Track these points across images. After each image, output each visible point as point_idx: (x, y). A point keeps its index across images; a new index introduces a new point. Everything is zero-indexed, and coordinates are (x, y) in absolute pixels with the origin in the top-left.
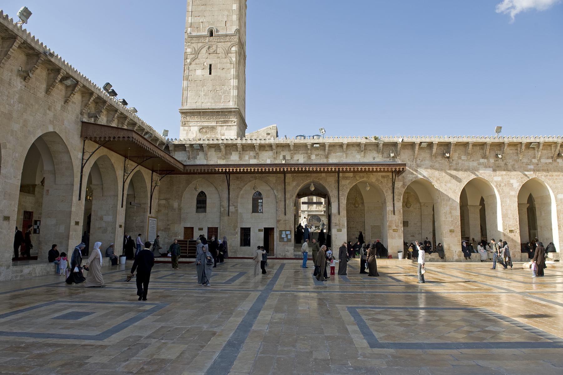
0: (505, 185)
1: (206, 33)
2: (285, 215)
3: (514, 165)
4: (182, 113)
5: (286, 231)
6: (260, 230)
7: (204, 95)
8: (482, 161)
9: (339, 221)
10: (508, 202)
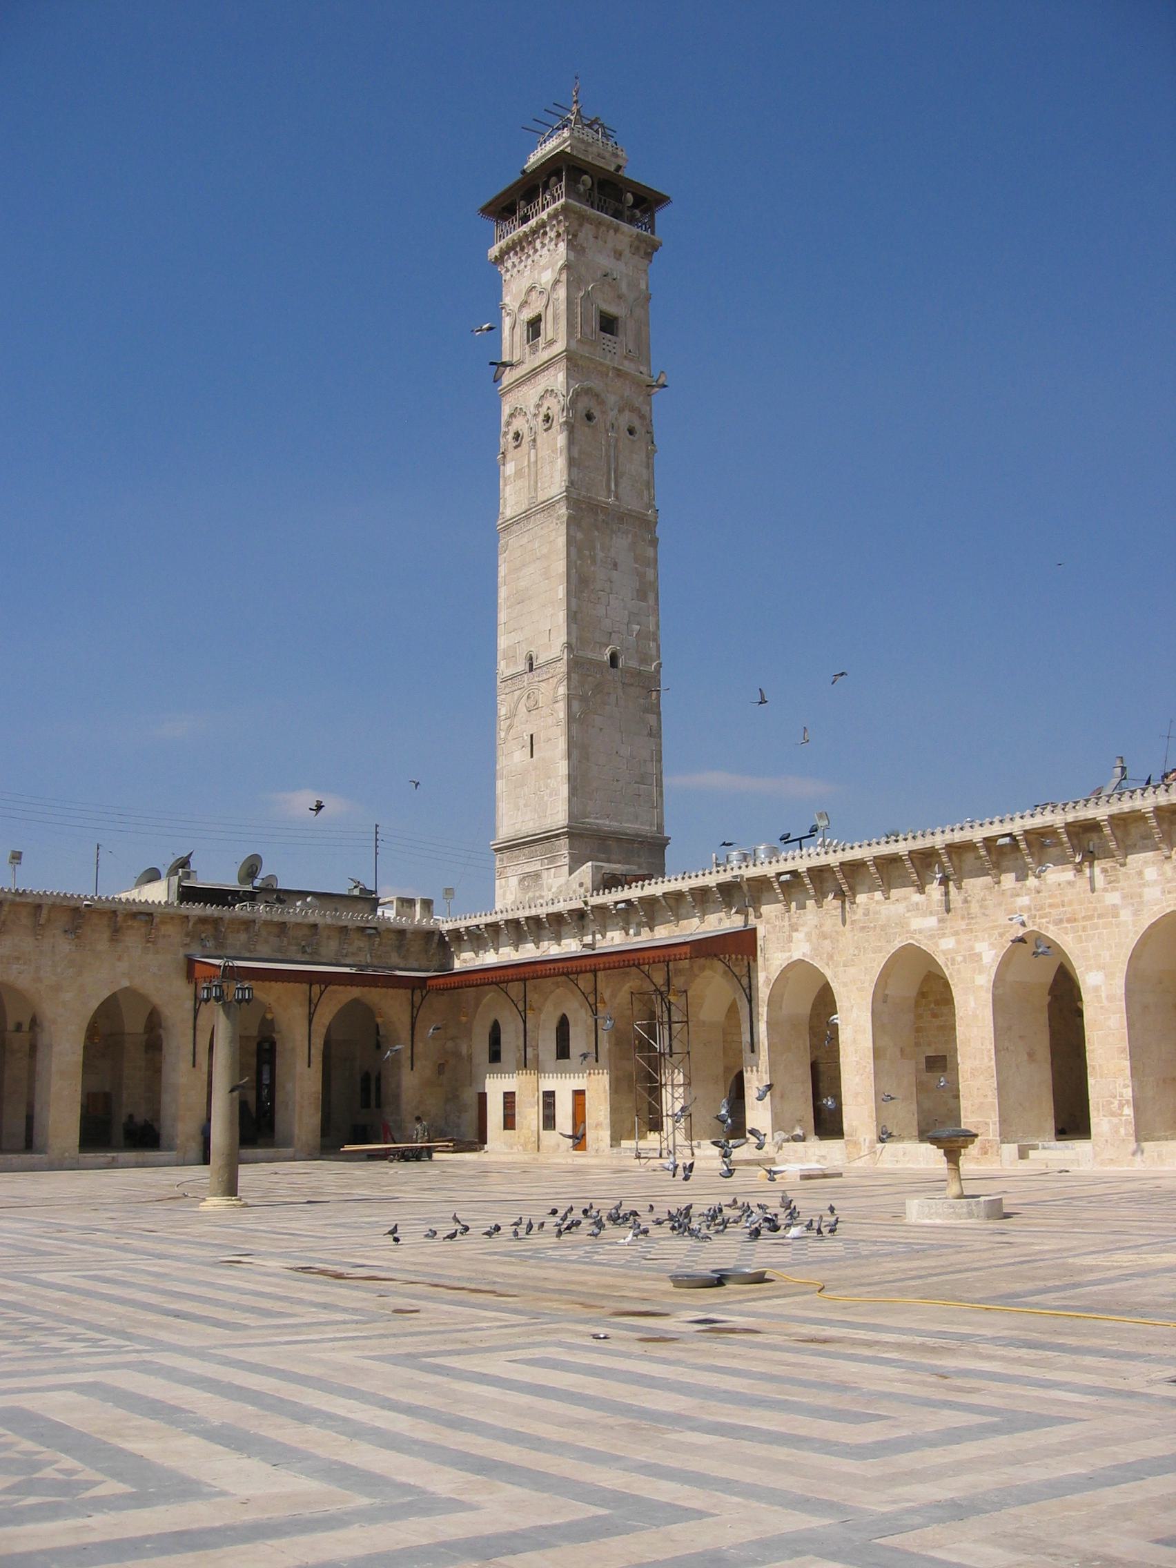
0: (965, 960)
1: (522, 666)
3: (984, 900)
7: (525, 806)
8: (917, 897)
10: (972, 1004)
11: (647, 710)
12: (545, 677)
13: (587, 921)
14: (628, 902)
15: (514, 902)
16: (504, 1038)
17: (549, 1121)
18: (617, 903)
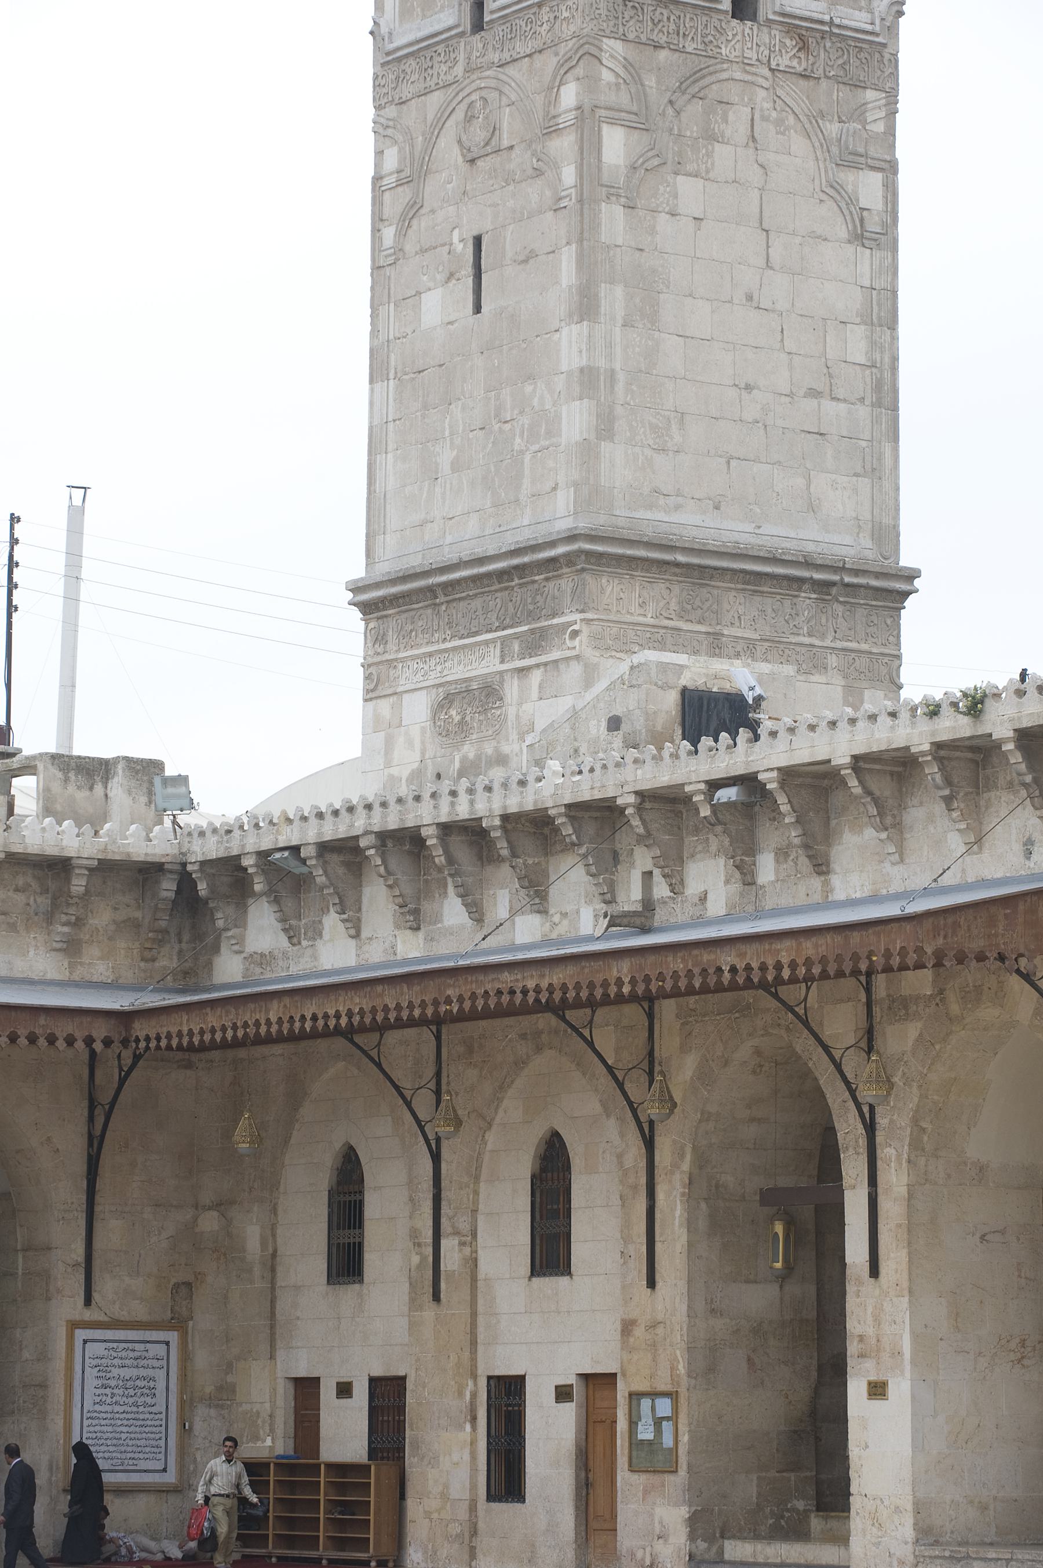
2: (651, 1283)
4: (367, 608)
5: (654, 1395)
6: (563, 1394)
7: (456, 467)
9: (877, 1321)
11: (852, 159)
12: (521, 48)
13: (623, 840)
14: (748, 781)
15: (417, 775)
16: (373, 1207)
17: (507, 1478)
18: (715, 785)
